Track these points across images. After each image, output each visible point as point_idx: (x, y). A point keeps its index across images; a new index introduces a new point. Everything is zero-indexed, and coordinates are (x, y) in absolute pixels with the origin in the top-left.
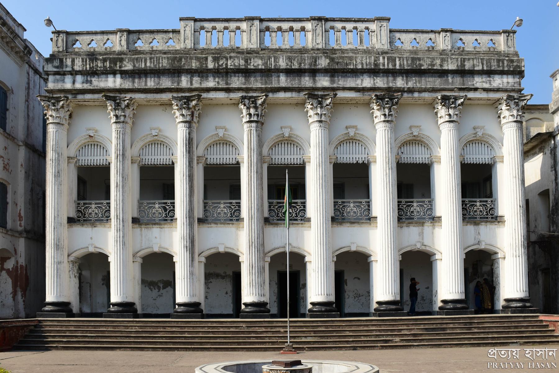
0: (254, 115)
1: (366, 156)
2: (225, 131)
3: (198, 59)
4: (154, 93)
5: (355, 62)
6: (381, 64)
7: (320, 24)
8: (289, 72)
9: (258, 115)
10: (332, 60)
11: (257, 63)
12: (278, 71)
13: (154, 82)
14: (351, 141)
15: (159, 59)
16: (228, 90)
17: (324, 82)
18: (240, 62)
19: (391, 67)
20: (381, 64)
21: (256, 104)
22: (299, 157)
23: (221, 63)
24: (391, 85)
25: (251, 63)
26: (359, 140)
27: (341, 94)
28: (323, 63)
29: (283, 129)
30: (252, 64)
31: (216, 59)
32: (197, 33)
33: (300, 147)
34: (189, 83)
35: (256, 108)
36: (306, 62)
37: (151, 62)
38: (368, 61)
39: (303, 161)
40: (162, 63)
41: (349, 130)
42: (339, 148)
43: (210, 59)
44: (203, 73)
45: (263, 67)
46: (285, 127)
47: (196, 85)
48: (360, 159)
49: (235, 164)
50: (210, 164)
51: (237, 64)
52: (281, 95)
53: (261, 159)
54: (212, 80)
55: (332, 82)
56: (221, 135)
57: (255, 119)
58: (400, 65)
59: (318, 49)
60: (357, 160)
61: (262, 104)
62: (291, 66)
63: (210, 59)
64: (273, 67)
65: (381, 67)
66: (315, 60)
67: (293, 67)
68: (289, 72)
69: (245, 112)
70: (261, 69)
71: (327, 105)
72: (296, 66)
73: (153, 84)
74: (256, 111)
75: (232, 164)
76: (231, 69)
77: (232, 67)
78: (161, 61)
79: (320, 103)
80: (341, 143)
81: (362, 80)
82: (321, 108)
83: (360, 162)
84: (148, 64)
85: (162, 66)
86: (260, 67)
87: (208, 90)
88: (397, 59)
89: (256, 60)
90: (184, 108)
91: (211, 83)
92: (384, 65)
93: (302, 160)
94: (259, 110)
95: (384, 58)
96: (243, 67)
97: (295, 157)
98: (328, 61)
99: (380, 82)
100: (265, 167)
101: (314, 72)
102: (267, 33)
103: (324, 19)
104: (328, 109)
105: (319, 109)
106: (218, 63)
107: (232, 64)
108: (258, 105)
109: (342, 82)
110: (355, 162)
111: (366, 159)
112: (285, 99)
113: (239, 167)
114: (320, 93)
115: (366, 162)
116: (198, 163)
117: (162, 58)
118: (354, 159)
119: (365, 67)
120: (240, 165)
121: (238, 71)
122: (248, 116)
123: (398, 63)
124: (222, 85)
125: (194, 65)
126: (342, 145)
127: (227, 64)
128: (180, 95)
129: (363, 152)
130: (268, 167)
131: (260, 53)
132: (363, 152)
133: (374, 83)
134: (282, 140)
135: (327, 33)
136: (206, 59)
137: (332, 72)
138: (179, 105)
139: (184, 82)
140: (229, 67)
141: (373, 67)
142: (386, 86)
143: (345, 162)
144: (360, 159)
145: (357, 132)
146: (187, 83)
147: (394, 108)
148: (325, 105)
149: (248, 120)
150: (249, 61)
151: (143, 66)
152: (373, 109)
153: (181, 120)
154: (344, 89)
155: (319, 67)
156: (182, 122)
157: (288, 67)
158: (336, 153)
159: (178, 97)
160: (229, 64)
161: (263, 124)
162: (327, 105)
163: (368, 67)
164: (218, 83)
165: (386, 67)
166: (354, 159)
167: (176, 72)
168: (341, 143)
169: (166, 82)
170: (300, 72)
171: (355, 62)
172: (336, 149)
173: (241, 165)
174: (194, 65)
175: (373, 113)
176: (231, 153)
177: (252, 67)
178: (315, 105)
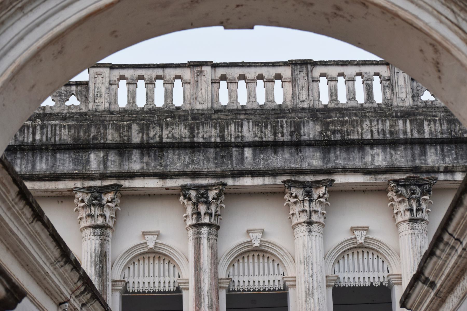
0: (205, 214)
1: (386, 274)
2: (157, 239)
3: (118, 129)
4: (45, 181)
5: (360, 130)
6: (401, 132)
7: (305, 70)
8: (259, 146)
9: (210, 215)
10: (326, 126)
11: (209, 133)
12: (242, 145)
13: (47, 164)
14: (360, 250)
15: (55, 129)
16: (163, 176)
17: (313, 159)
18: (181, 132)
19: (416, 135)
20: (401, 132)
21: (207, 197)
22: (277, 278)
23: (152, 134)
24: (418, 162)
25: (198, 133)
26: (373, 249)
27: (340, 179)
28: (311, 131)
29: (251, 234)
30: (200, 135)
31: (144, 129)
32: (114, 87)
33: (278, 262)
34: (102, 166)
35: (208, 204)
36: (285, 131)
37: (42, 134)
38: (380, 127)
39: (284, 284)
40: (60, 135)
41: (356, 233)
42: (341, 262)
43: (135, 127)
44: (123, 149)
45: (218, 140)
46: (254, 231)
47: (113, 168)
48: (376, 280)
49: (174, 292)
50: (133, 292)
51: (177, 136)
52: (247, 181)
53: (217, 282)
54: (138, 160)
55: (325, 159)
56: (151, 245)
57: (206, 220)
58: (431, 133)
59: (303, 109)
60: (372, 280)
61: (216, 198)
62: (262, 138)
63: (135, 127)
64: (233, 140)
65: (402, 136)
66: (297, 127)
67: (264, 139)
68: (259, 146)
69: (189, 210)
70: (216, 143)
71: (319, 197)
72: (269, 137)
73: (44, 166)
74: (208, 208)
75: (170, 292)
76: (167, 143)
77: (169, 140)
78: (58, 132)
79: (309, 194)
80: (344, 254)
81: (373, 156)
82: (311, 201)
83: (377, 283)
84: (38, 137)
85: (60, 139)
86: (213, 140)
87: (132, 176)
88: (426, 123)
89: (207, 128)
90: (94, 205)
91: (136, 166)
92: (405, 133)
93: (282, 283)
94: (213, 208)
95: (405, 123)
96: (187, 140)
97: (272, 278)
98: (318, 128)
99: (401, 158)
100: (223, 295)
101: (297, 145)
102: (223, 83)
103: (310, 63)
104: (321, 202)
105: (307, 204)
106: (148, 134)
107: (170, 135)
108: (210, 199)
109: (340, 159)
110: (368, 284)
111: (386, 280)
112: (253, 186)
113: (181, 296)
114: (309, 178)
115: (386, 284)
116: (113, 290)
117: (60, 127)
118: (367, 280)
119: (376, 136)
120: (181, 292)
121: (178, 146)
122: (195, 216)
123: (427, 129)
124: (153, 166)
125: (111, 136)
126: (346, 257)
127: (161, 137)
128: (88, 184)
129: (381, 269)
130: (227, 295)
131: (213, 117)
132: (381, 269)
133: (392, 160)
134: (249, 251)
135: (315, 84)
136: (130, 127)
137: (326, 145)
138: (86, 201)
139: (94, 161)
140: (165, 140)
141: (388, 136)
142: (410, 164)
143: (352, 284)
144: (376, 280)
145: (368, 236)
146: (99, 166)
147: (425, 200)
148: (315, 197)
149: (194, 222)
150: (196, 131)
151: (30, 140)
152: (393, 200)
153: (88, 224)
154: (345, 171)
155: (306, 138)
156: (90, 227)
157: (257, 139)
158: (336, 270)
159: (84, 188)
160: (165, 136)
161: (218, 228)
162: (319, 197)
163: (381, 137)
164: (147, 164)
165: (409, 136)
166: (367, 280)
167: (80, 147)
168: (344, 254)
169: (66, 163)
170: (276, 146)
171: (360, 130)
172: (336, 266)
173: (184, 293)
174: (109, 137)
175: (392, 205)
176: (167, 274)
177: (201, 140)
178: (300, 198)
